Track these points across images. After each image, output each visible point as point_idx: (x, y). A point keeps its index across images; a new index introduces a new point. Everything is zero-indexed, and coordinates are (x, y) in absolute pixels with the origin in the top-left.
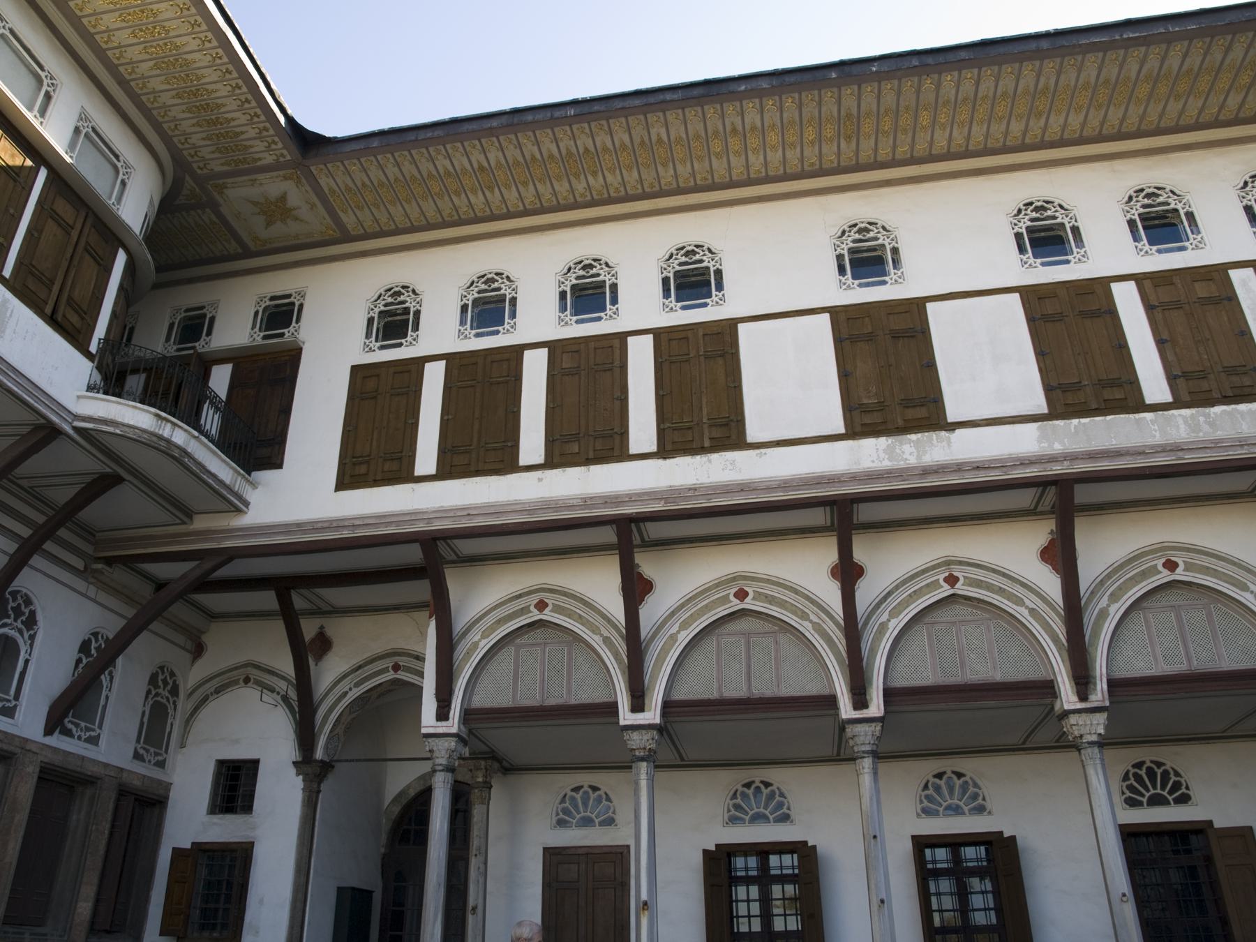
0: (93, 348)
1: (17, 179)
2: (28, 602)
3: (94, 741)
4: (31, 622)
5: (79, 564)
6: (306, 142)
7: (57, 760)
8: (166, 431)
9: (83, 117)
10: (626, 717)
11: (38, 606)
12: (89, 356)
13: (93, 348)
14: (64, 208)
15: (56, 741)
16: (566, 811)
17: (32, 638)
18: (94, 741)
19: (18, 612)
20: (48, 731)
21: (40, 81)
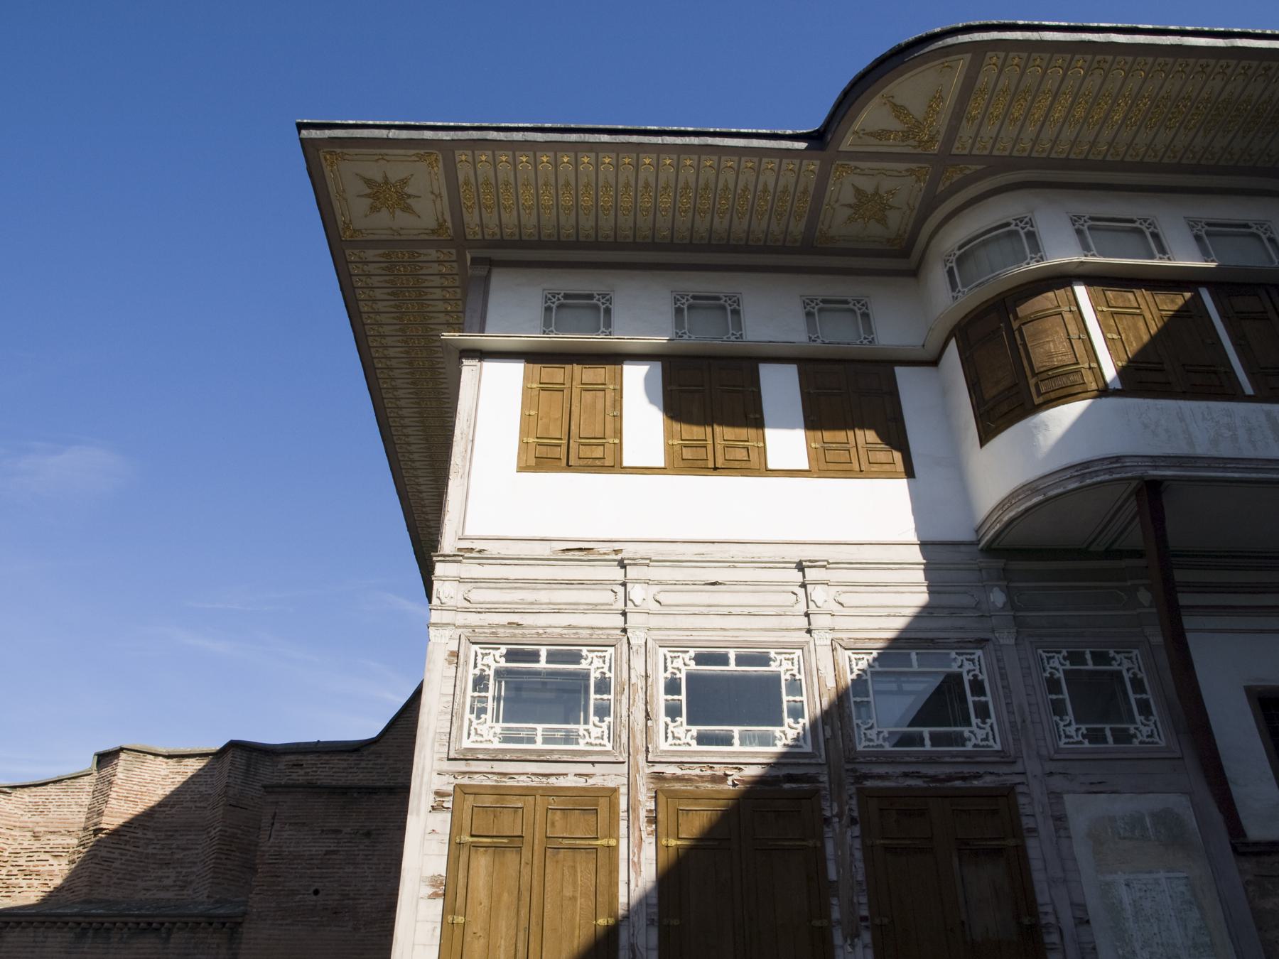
1: (1190, 315)
9: (1192, 224)
21: (1140, 232)
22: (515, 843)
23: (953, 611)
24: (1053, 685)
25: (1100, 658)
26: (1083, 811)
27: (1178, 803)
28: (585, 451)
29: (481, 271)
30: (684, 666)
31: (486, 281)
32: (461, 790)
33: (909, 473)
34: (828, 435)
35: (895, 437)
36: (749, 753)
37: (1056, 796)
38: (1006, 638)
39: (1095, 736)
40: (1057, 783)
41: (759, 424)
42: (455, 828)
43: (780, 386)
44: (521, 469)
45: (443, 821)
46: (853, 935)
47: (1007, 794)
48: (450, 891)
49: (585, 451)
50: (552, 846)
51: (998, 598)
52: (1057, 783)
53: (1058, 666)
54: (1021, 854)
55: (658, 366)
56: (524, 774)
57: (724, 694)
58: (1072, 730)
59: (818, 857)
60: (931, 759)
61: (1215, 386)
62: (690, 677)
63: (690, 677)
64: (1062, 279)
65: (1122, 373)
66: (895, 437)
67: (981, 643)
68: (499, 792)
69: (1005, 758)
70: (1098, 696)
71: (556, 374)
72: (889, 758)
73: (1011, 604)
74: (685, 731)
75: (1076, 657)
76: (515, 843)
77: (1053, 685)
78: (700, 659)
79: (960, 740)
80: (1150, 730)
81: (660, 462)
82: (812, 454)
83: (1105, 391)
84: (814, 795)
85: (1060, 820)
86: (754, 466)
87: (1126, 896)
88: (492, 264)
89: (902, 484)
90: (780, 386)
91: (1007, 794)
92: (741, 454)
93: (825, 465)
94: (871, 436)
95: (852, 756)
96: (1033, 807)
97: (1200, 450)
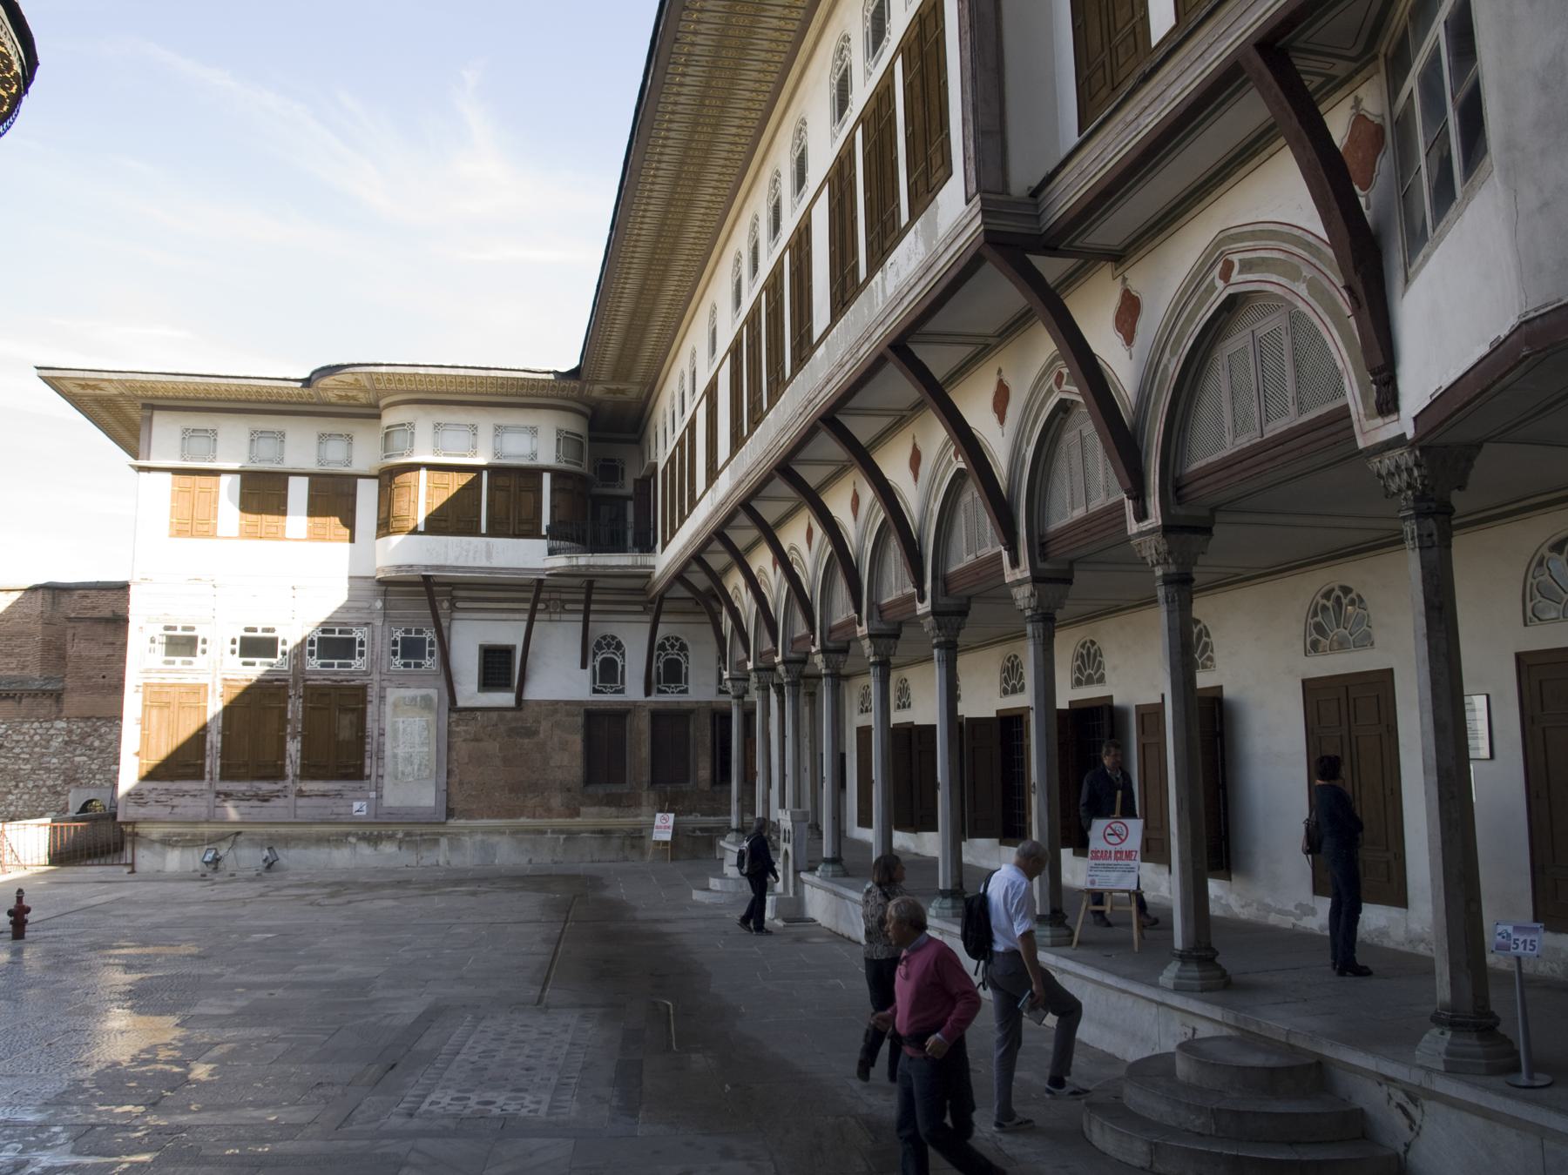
0: (544, 532)
1: (472, 488)
2: (613, 638)
3: (685, 691)
4: (619, 646)
5: (640, 608)
6: (574, 374)
7: (660, 707)
8: (574, 562)
10: (750, 665)
11: (620, 638)
12: (544, 537)
13: (544, 532)
14: (501, 481)
15: (653, 698)
16: (1319, 628)
17: (623, 655)
18: (685, 691)
19: (609, 645)
20: (648, 694)
22: (168, 705)
23: (358, 609)
24: (395, 643)
25: (419, 632)
26: (393, 694)
27: (433, 693)
28: (200, 528)
29: (147, 413)
30: (239, 633)
31: (150, 419)
32: (146, 685)
33: (352, 540)
34: (317, 520)
35: (349, 522)
36: (258, 669)
37: (383, 689)
38: (378, 623)
39: (406, 665)
40: (385, 684)
41: (284, 513)
42: (144, 699)
43: (298, 491)
44: (171, 536)
45: (140, 696)
46: (294, 738)
47: (364, 688)
48: (144, 723)
49: (200, 528)
50: (182, 707)
51: (379, 604)
52: (385, 684)
53: (399, 635)
54: (363, 712)
55: (238, 478)
56: (171, 679)
57: (253, 646)
58: (398, 661)
59: (285, 710)
60: (336, 673)
61: (471, 530)
62: (243, 639)
63: (243, 639)
64: (415, 467)
65: (428, 520)
66: (349, 522)
67: (367, 624)
68: (161, 685)
69: (365, 673)
70: (411, 649)
71: (187, 480)
72: (318, 673)
73: (385, 607)
74: (237, 660)
75: (408, 631)
76: (168, 705)
77: (395, 643)
78: (247, 630)
79: (350, 666)
80: (431, 663)
81: (236, 534)
82: (309, 530)
83: (414, 532)
84: (286, 687)
85: (382, 698)
86: (278, 536)
87: (401, 726)
88: (154, 407)
89: (348, 544)
90: (298, 491)
91: (364, 688)
92: (273, 530)
93: (314, 536)
94: (337, 520)
95: (303, 671)
96: (372, 694)
97: (449, 563)
